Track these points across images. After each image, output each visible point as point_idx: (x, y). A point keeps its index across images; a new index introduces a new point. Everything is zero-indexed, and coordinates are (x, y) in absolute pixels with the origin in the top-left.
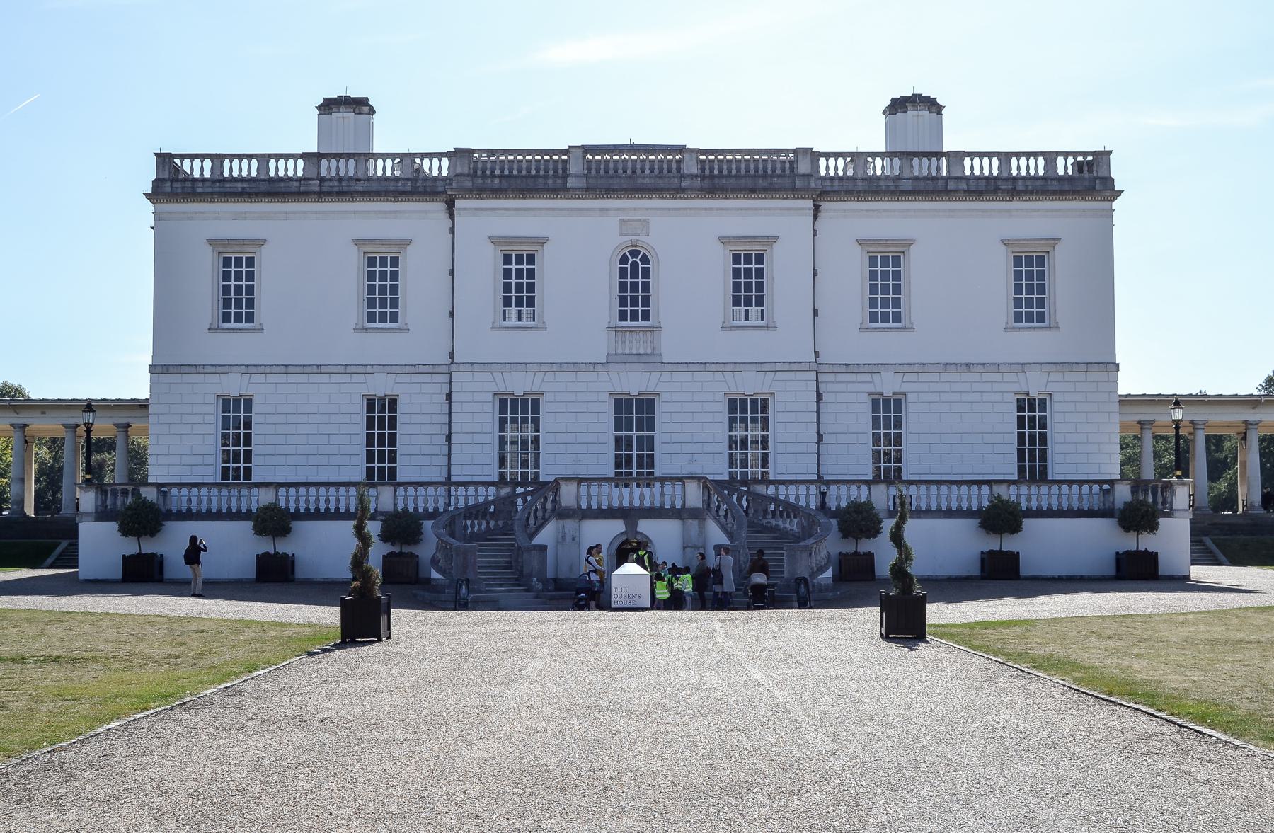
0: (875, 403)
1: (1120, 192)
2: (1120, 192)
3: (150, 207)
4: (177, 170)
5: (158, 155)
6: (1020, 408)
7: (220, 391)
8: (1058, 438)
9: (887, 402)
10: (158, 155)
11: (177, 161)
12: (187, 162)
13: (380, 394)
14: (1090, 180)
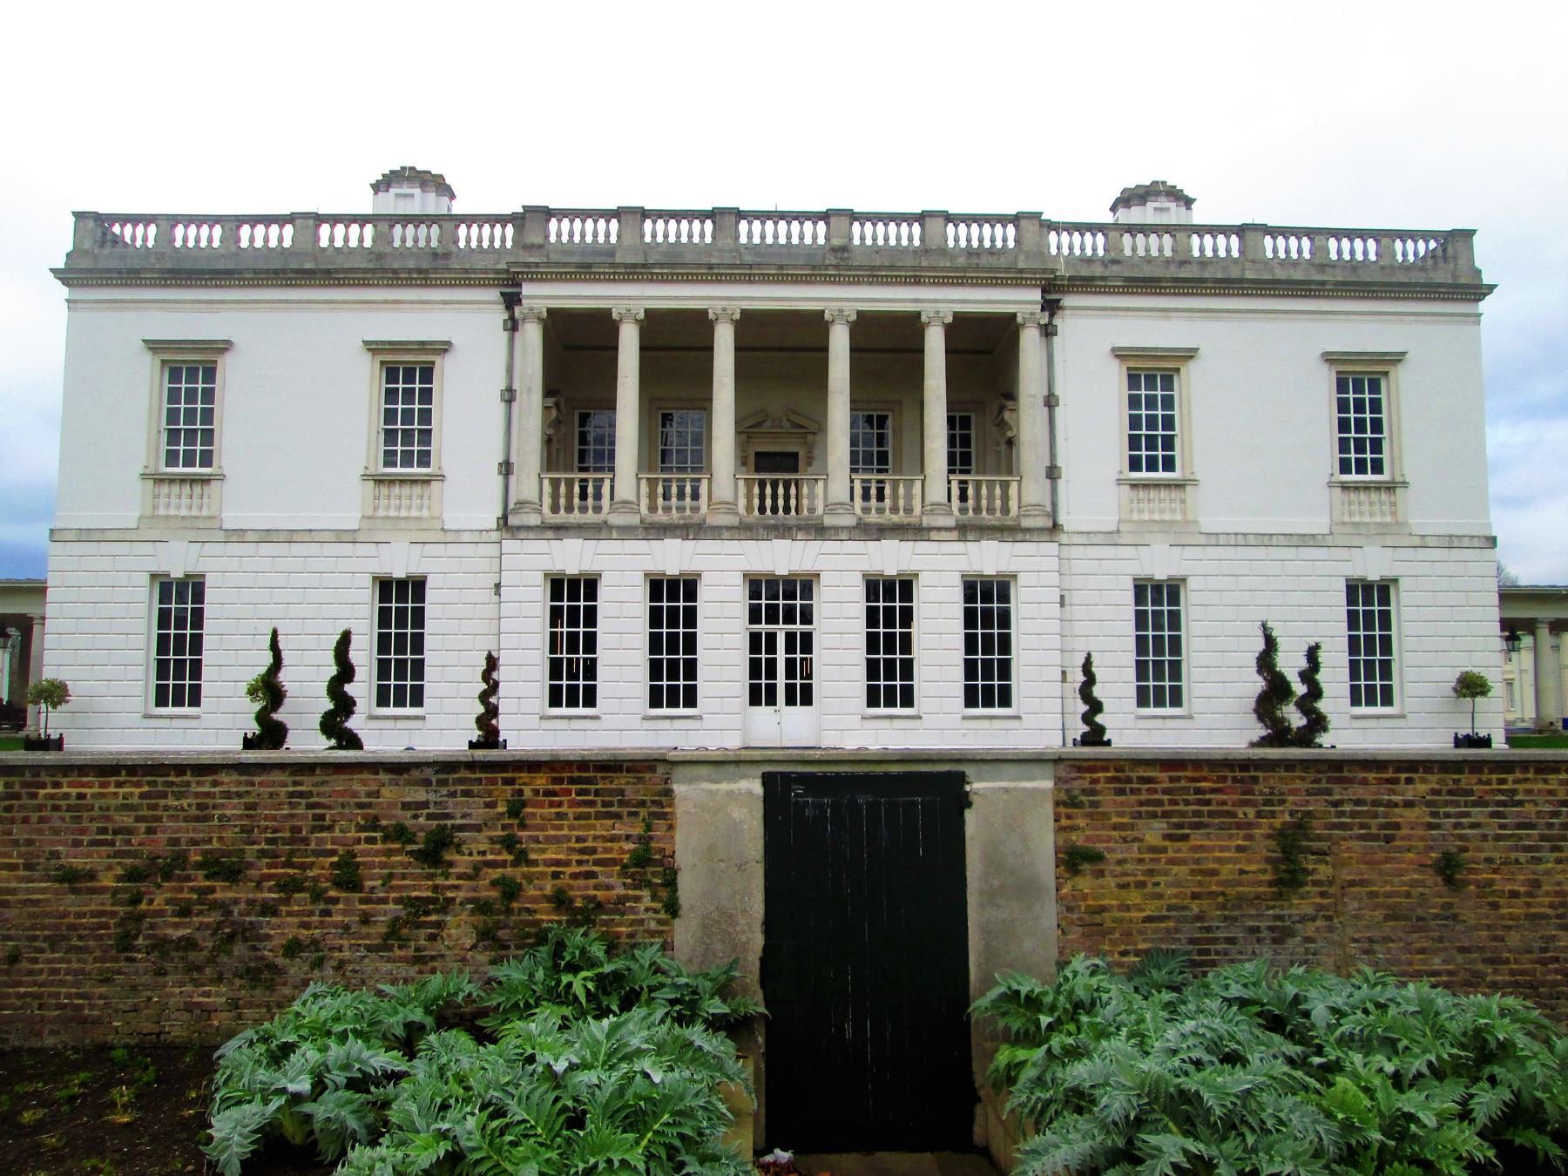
0: (1140, 590)
1: (1492, 288)
2: (1492, 288)
3: (65, 292)
4: (117, 241)
5: (79, 216)
6: (1351, 600)
7: (154, 568)
8: (1409, 643)
9: (1157, 588)
10: (79, 216)
11: (116, 229)
12: (128, 229)
13: (399, 573)
14: (1443, 275)
